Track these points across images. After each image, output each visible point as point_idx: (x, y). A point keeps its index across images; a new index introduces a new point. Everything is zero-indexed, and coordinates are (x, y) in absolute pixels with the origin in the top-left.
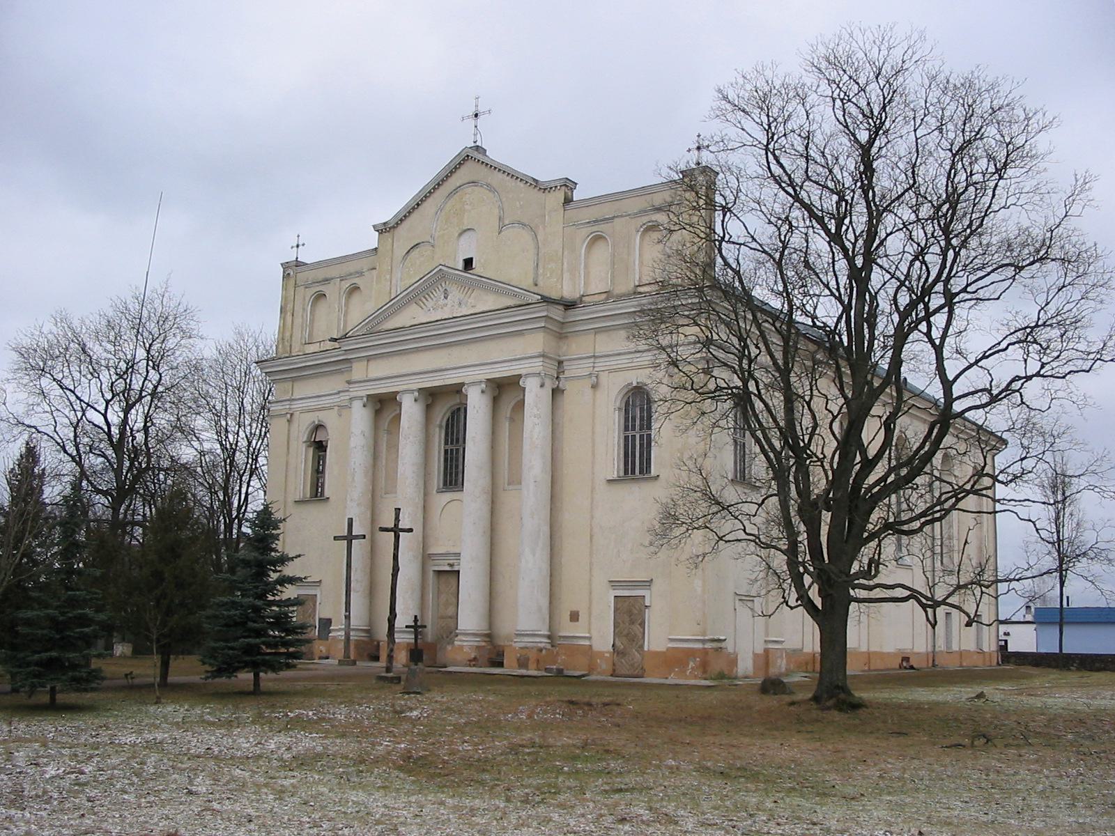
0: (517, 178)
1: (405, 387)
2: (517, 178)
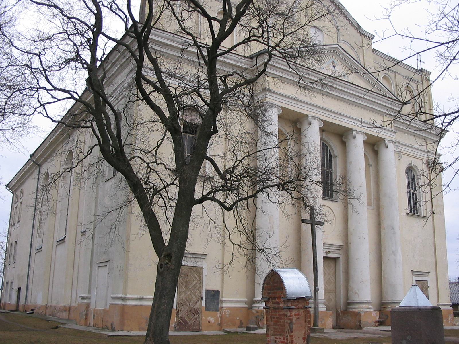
1: (313, 115)
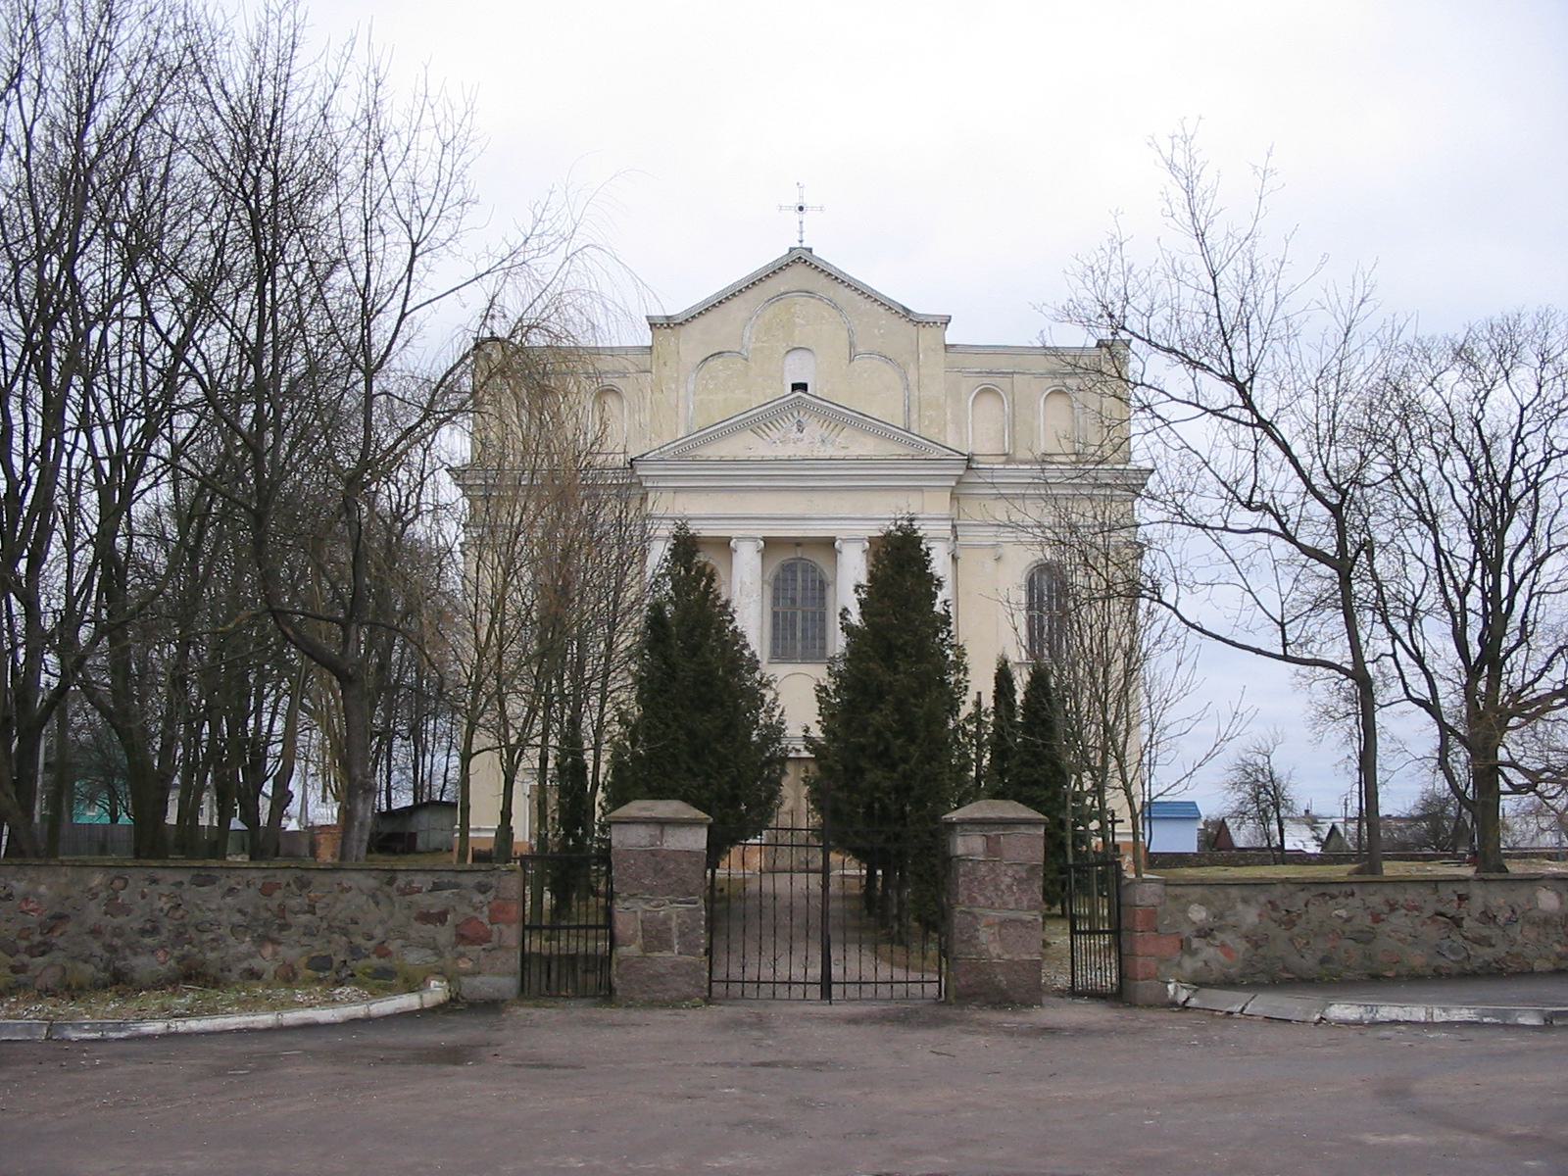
0: (876, 300)
2: (876, 300)
